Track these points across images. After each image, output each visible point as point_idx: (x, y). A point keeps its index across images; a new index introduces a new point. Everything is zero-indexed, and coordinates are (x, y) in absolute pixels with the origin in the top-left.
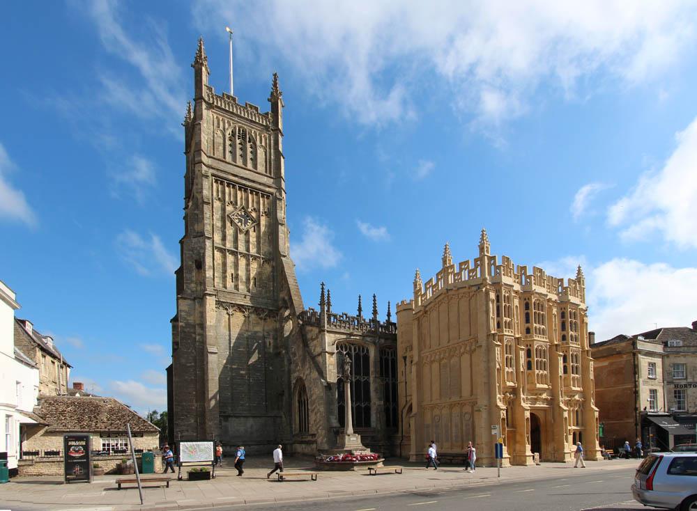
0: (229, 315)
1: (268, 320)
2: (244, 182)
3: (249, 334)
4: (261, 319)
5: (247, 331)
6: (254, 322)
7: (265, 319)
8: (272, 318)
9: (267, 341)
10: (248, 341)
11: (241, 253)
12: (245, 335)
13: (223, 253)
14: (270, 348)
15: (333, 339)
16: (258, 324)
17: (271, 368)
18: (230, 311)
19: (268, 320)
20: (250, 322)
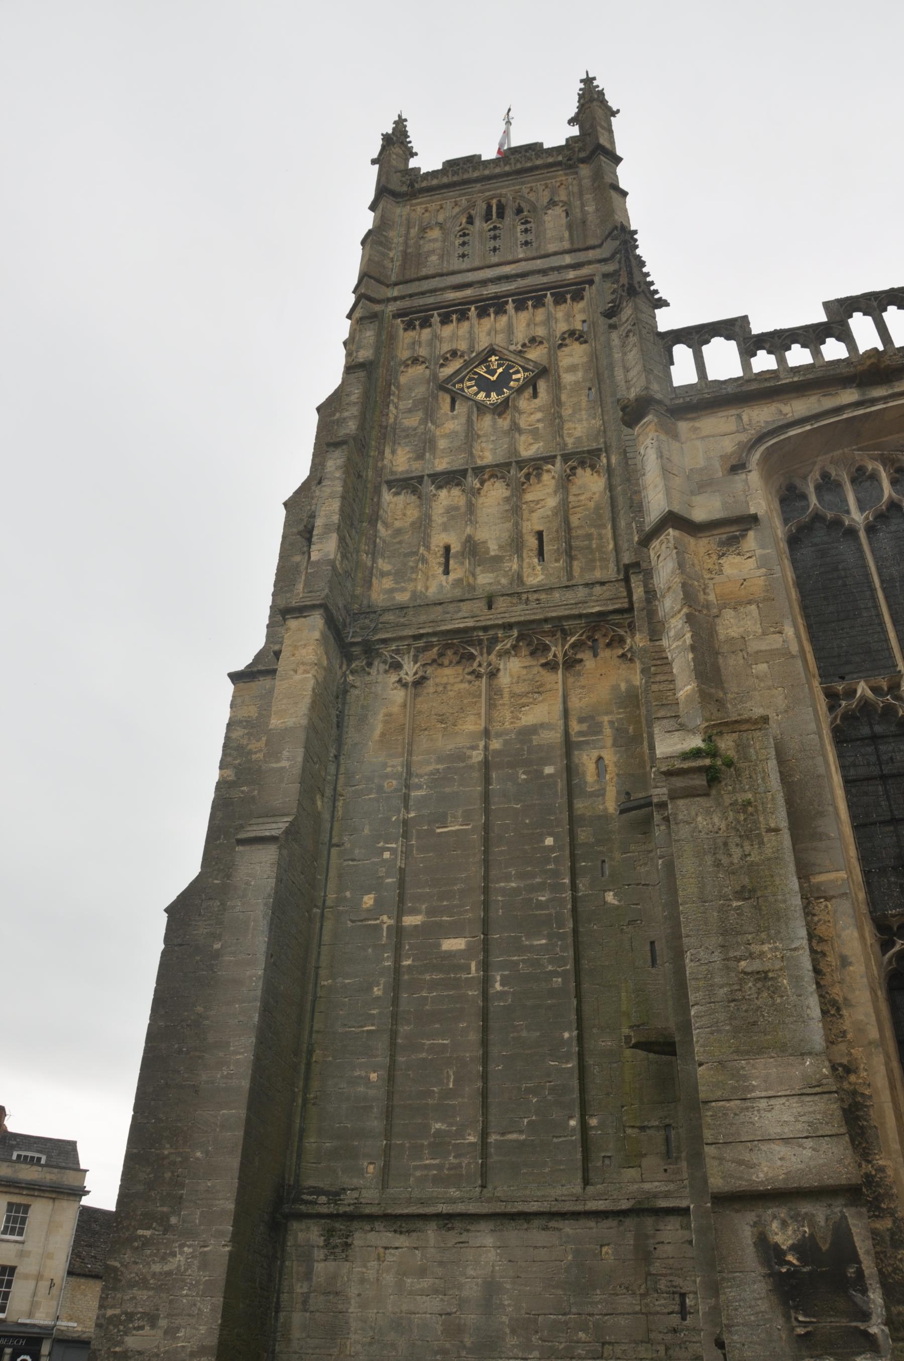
0: (405, 685)
1: (589, 663)
2: (492, 290)
3: (496, 745)
4: (551, 666)
5: (487, 733)
6: (520, 689)
7: (571, 664)
8: (605, 654)
9: (586, 760)
10: (487, 781)
11: (479, 471)
12: (477, 756)
13: (415, 491)
14: (601, 793)
15: (728, 445)
16: (539, 690)
17: (610, 897)
18: (410, 670)
19: (589, 663)
20: (499, 692)
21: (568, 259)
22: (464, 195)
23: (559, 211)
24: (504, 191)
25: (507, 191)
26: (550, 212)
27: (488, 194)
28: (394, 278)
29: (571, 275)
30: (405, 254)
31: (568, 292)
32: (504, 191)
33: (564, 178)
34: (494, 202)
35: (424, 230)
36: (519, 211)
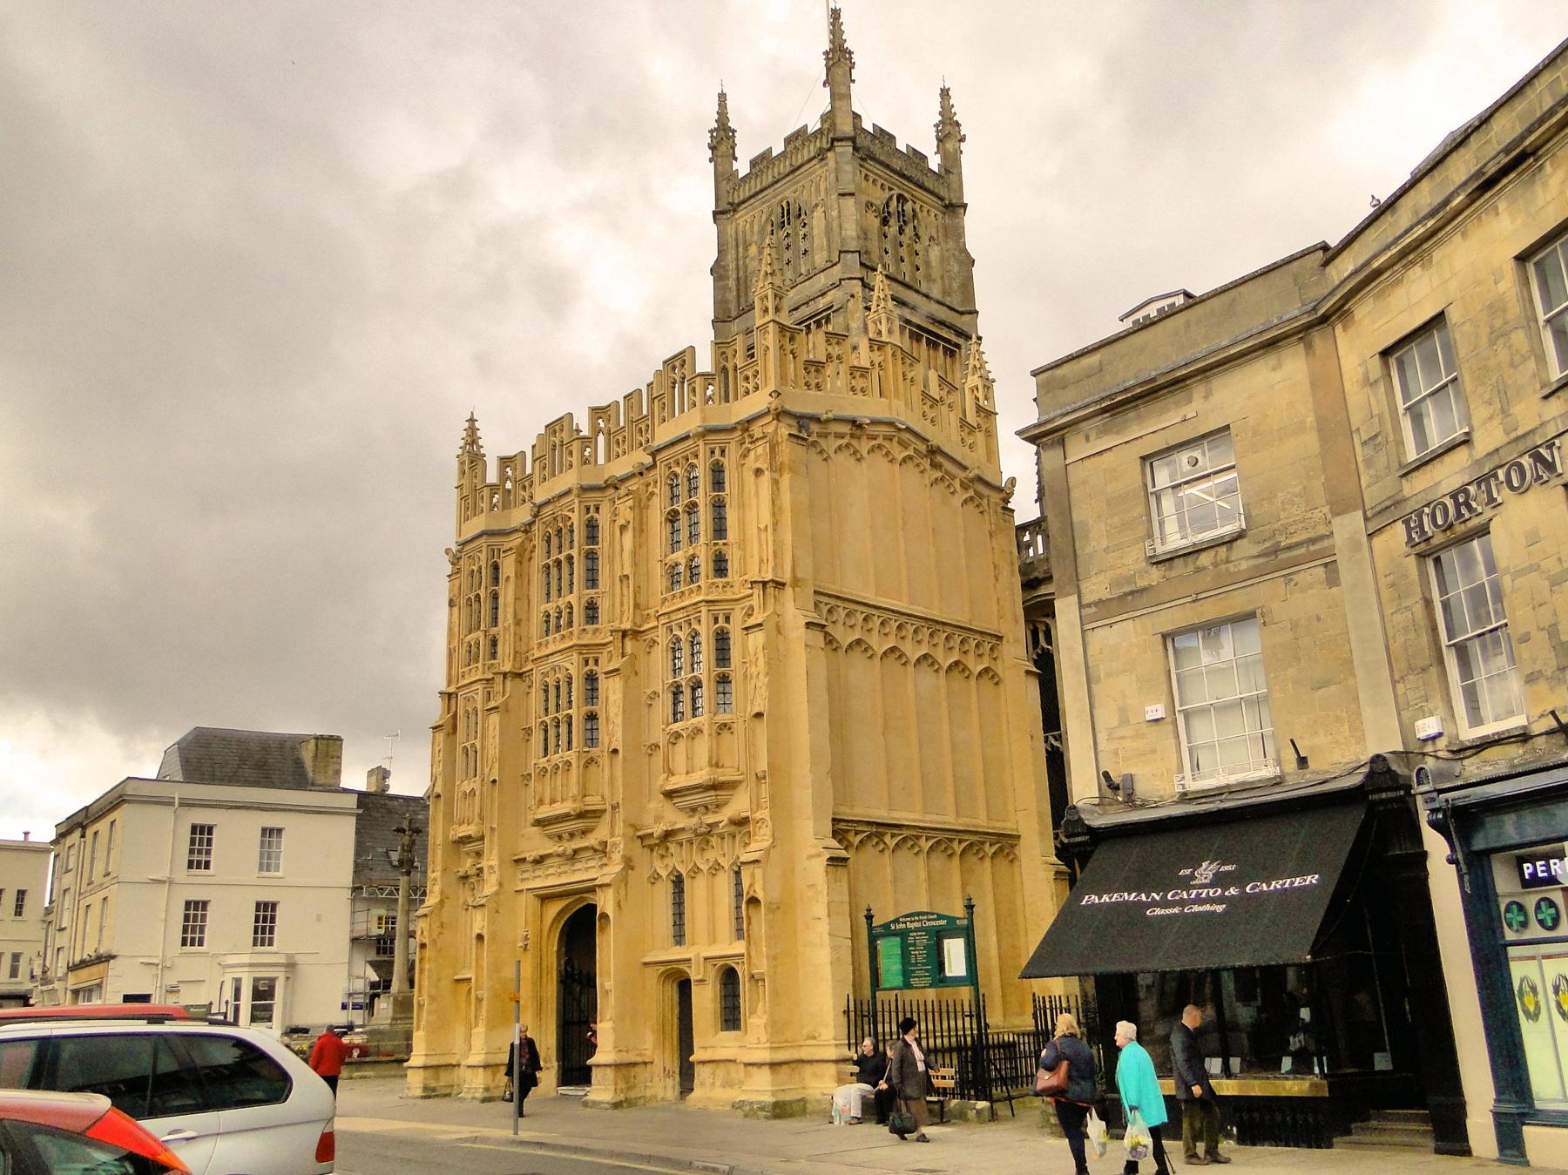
21: (822, 280)
22: (764, 203)
23: (820, 210)
24: (787, 193)
25: (787, 192)
26: (815, 214)
27: (779, 198)
28: (734, 314)
29: (822, 303)
30: (738, 279)
31: (822, 318)
32: (787, 193)
33: (821, 171)
34: (784, 204)
35: (746, 249)
36: (800, 215)
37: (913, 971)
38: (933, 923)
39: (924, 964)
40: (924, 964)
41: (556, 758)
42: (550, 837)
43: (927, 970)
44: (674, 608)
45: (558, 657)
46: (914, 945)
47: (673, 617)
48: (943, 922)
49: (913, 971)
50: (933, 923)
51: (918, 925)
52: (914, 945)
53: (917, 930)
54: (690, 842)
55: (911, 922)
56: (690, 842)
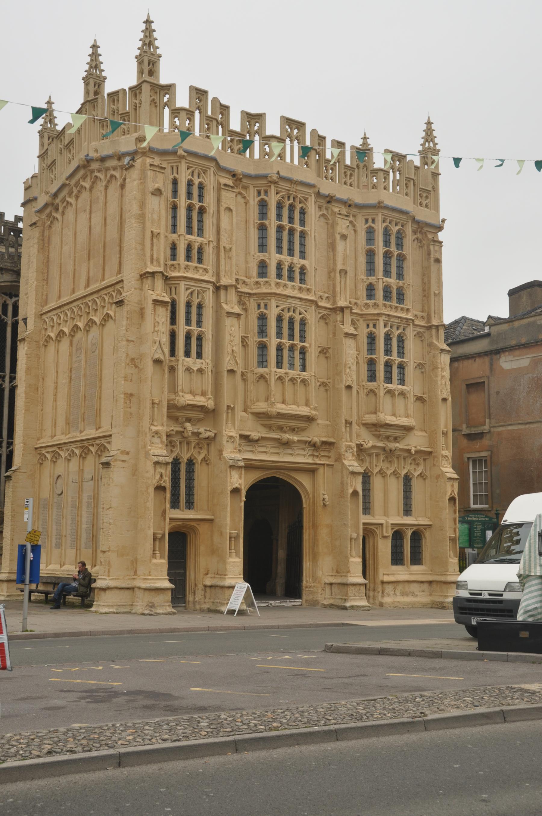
37: (475, 540)
38: (483, 519)
39: (480, 537)
40: (480, 537)
41: (293, 373)
42: (264, 426)
43: (481, 540)
44: (396, 314)
45: (297, 302)
46: (476, 528)
47: (392, 320)
48: (487, 519)
49: (475, 540)
50: (483, 519)
51: (477, 519)
52: (476, 528)
53: (477, 521)
54: (377, 455)
55: (475, 517)
56: (377, 455)
